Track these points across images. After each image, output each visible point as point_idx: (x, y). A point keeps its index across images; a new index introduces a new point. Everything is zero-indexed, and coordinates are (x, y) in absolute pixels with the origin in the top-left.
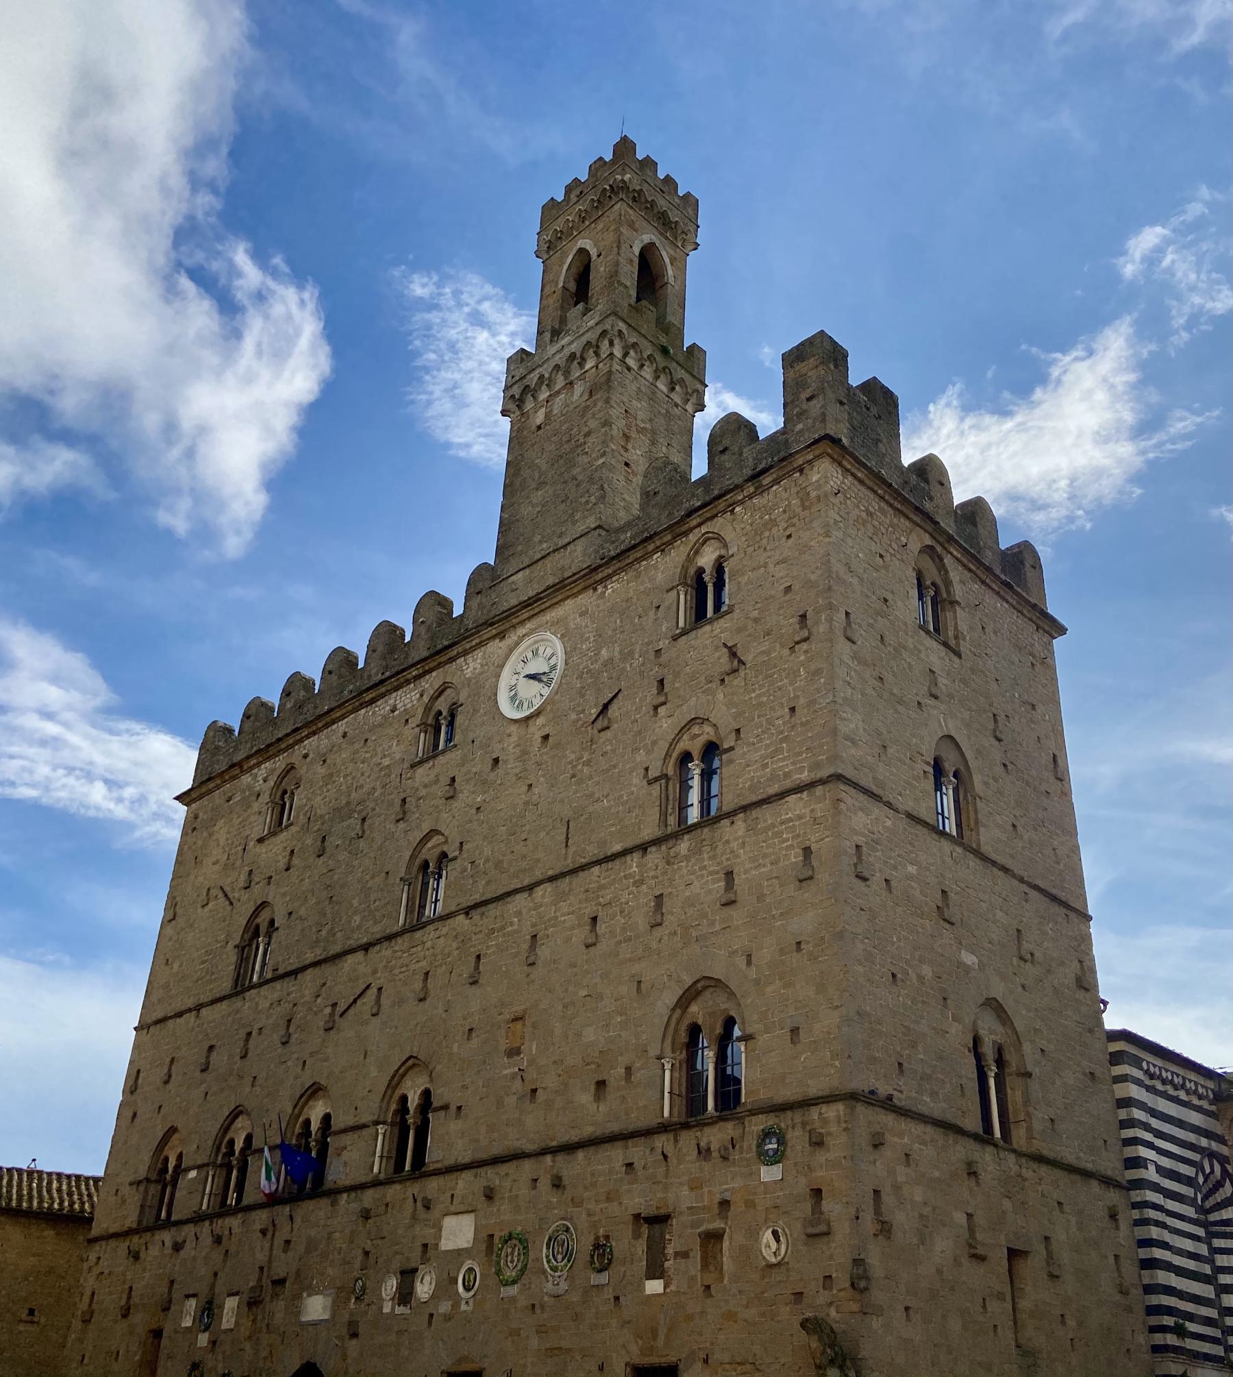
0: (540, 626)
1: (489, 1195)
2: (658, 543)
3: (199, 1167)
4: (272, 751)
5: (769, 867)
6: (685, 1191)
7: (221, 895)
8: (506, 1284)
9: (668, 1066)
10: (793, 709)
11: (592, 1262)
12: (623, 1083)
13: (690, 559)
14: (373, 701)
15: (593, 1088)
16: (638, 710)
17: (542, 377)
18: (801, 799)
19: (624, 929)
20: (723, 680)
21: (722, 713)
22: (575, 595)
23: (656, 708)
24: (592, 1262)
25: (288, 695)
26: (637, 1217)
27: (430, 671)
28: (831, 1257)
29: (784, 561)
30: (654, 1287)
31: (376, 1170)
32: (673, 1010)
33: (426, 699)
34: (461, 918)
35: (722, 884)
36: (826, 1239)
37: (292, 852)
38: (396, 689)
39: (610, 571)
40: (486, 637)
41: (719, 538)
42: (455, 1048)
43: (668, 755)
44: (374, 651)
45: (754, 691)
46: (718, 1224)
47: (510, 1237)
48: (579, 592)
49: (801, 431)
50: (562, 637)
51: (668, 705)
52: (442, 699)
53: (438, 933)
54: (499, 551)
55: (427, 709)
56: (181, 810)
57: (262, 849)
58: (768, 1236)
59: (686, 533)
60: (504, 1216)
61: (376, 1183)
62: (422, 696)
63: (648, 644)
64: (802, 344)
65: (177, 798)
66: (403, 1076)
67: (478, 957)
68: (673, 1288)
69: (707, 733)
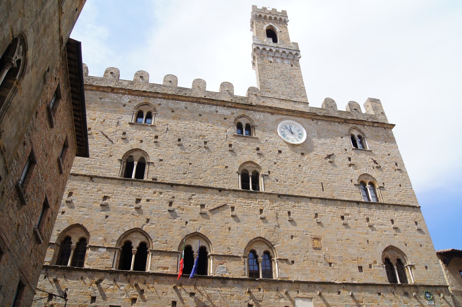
2: (339, 120)
14: (203, 103)
17: (271, 50)
22: (305, 118)
33: (235, 116)
34: (276, 196)
35: (390, 222)
38: (217, 105)
40: (266, 110)
41: (360, 131)
42: (286, 240)
48: (307, 118)
59: (348, 123)
62: (233, 114)
63: (341, 146)
66: (252, 243)
67: (289, 213)
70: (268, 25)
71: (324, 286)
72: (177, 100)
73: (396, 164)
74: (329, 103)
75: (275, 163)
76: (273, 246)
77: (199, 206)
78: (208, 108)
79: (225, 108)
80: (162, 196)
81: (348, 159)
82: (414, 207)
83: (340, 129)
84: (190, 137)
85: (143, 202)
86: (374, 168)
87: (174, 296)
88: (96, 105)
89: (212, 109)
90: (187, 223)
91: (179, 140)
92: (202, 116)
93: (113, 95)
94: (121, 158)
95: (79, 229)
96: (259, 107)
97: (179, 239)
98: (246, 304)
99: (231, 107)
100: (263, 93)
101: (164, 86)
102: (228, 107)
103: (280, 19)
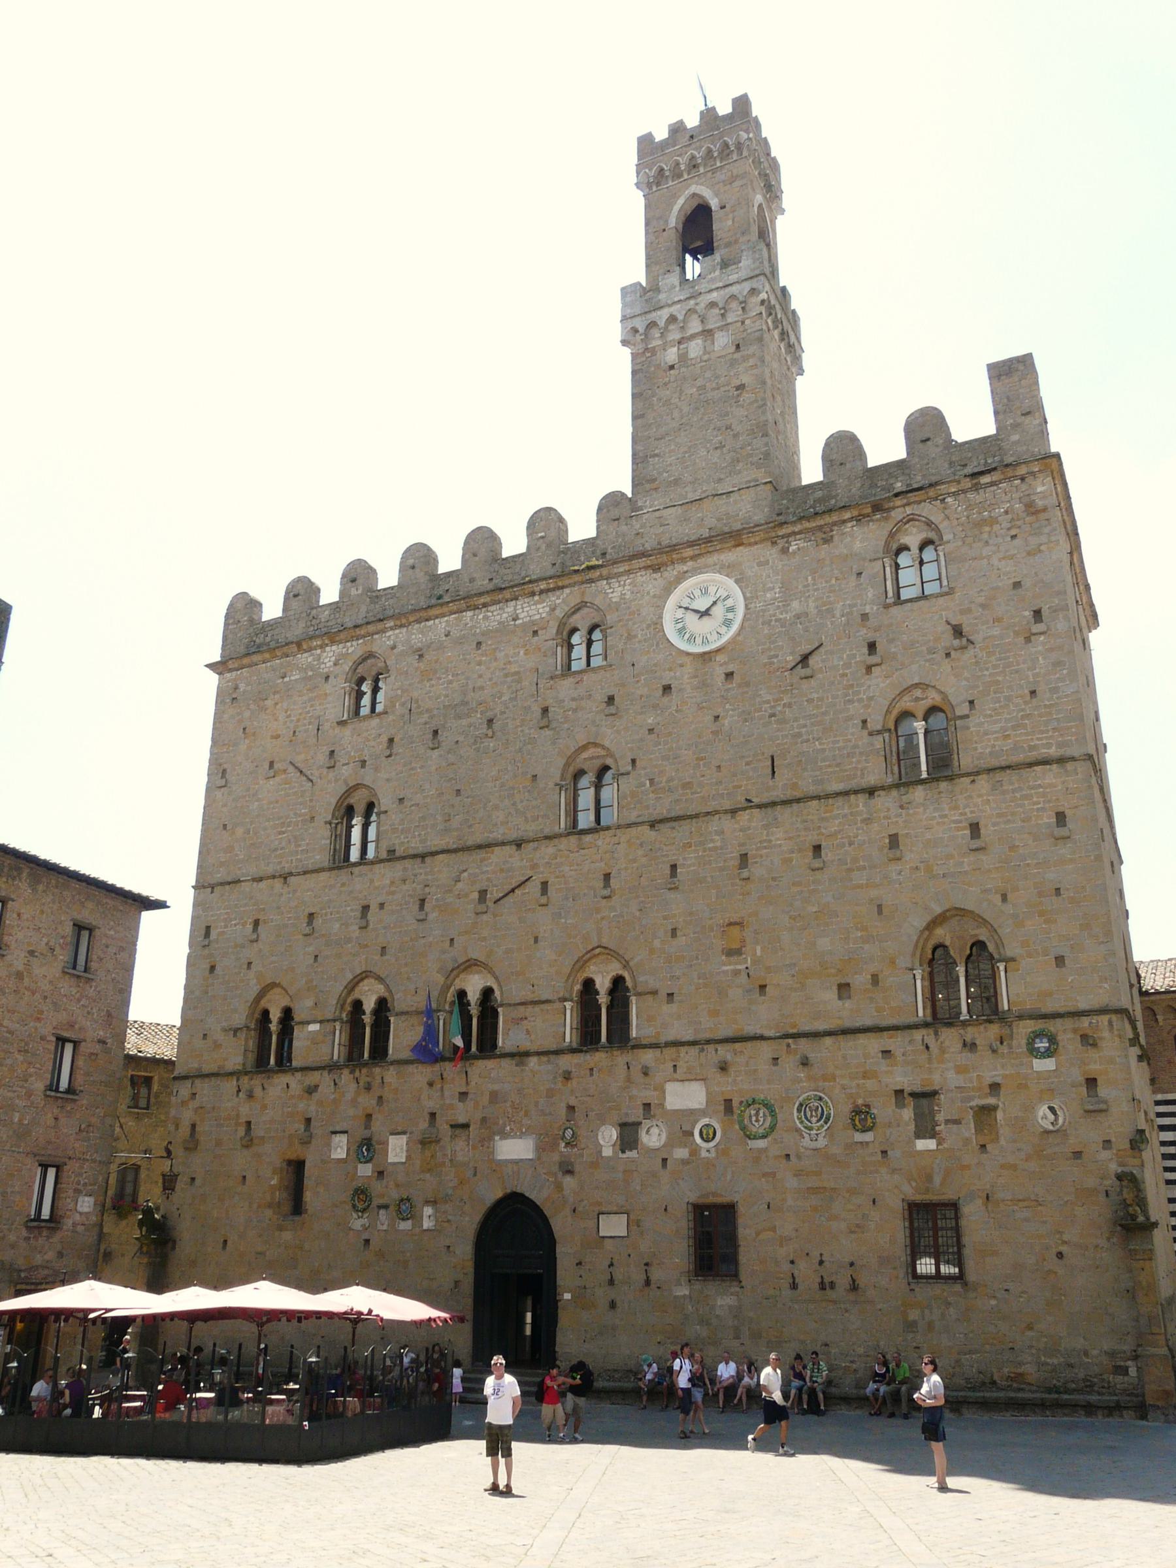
0: (706, 566)
1: (723, 1068)
2: (855, 513)
3: (321, 1022)
4: (342, 636)
5: (1020, 823)
6: (951, 1075)
7: (291, 769)
8: (755, 1137)
9: (918, 977)
10: (1033, 693)
11: (854, 1126)
12: (870, 986)
13: (892, 535)
14: (485, 605)
15: (835, 988)
16: (847, 665)
17: (672, 319)
18: (1050, 770)
19: (855, 860)
20: (948, 655)
21: (952, 684)
22: (750, 545)
23: (869, 669)
24: (854, 1126)
25: (353, 581)
26: (899, 1093)
27: (563, 587)
28: (1110, 1127)
29: (1012, 557)
30: (926, 1145)
31: (568, 1039)
32: (922, 932)
33: (559, 613)
34: (646, 828)
35: (968, 832)
36: (1104, 1114)
37: (391, 740)
38: (516, 599)
39: (797, 528)
41: (929, 524)
42: (657, 943)
43: (888, 712)
44: (475, 555)
45: (987, 669)
46: (991, 1101)
47: (754, 1101)
48: (756, 543)
49: (1018, 442)
50: (737, 582)
51: (883, 667)
52: (577, 617)
53: (616, 840)
54: (636, 484)
55: (562, 624)
56: (213, 679)
57: (347, 731)
58: (1043, 1110)
59: (889, 510)
60: (737, 1085)
61: (573, 1051)
64: (1011, 360)
65: (206, 666)
66: (586, 962)
67: (674, 867)
68: (945, 1145)
69: (933, 698)
70: (681, 201)
71: (737, 1046)
72: (427, 620)
73: (1037, 614)
74: (843, 449)
75: (651, 731)
76: (627, 962)
77: (476, 895)
78: (497, 615)
79: (536, 598)
80: (405, 887)
81: (865, 650)
82: (1061, 761)
83: (858, 545)
84: (458, 717)
85: (374, 908)
86: (948, 655)
87: (430, 1103)
88: (277, 696)
89: (505, 615)
90: (452, 940)
91: (436, 732)
92: (483, 647)
93: (305, 659)
94: (329, 818)
95: (277, 990)
96: (615, 563)
97: (441, 979)
98: (563, 1105)
99: (548, 590)
100: (640, 504)
101: (400, 586)
102: (542, 592)
103: (726, 145)
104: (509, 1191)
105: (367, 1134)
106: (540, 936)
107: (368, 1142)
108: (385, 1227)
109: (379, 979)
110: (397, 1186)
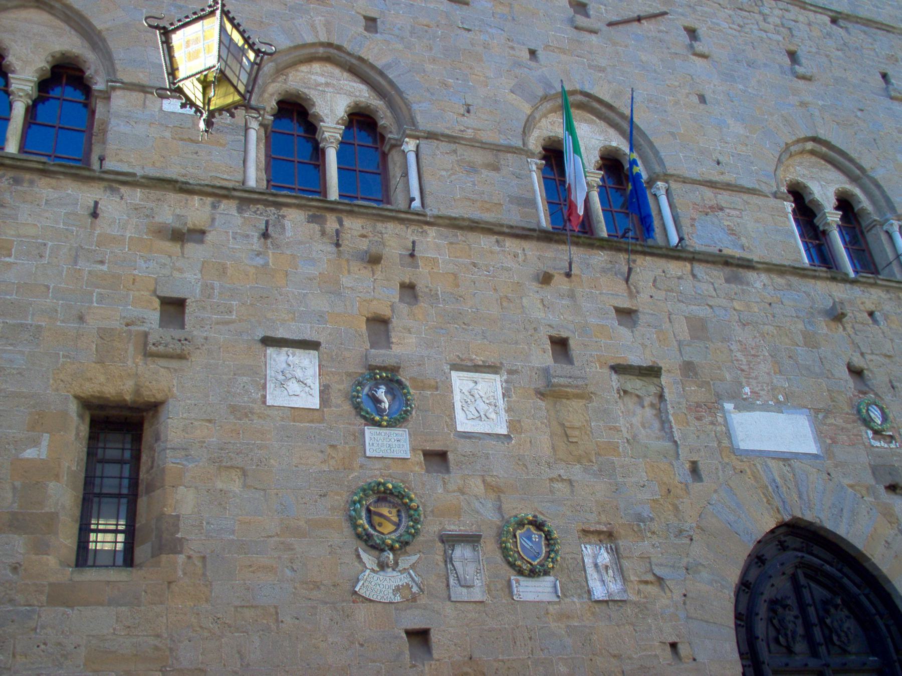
104: (787, 518)
105: (380, 356)
106: (709, 96)
107: (391, 378)
108: (478, 594)
109: (358, 69)
110: (495, 490)
